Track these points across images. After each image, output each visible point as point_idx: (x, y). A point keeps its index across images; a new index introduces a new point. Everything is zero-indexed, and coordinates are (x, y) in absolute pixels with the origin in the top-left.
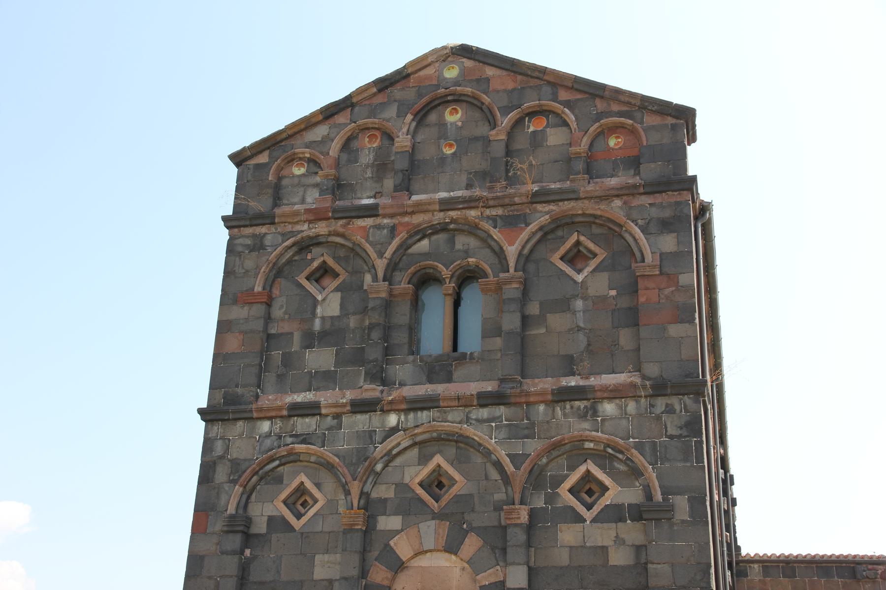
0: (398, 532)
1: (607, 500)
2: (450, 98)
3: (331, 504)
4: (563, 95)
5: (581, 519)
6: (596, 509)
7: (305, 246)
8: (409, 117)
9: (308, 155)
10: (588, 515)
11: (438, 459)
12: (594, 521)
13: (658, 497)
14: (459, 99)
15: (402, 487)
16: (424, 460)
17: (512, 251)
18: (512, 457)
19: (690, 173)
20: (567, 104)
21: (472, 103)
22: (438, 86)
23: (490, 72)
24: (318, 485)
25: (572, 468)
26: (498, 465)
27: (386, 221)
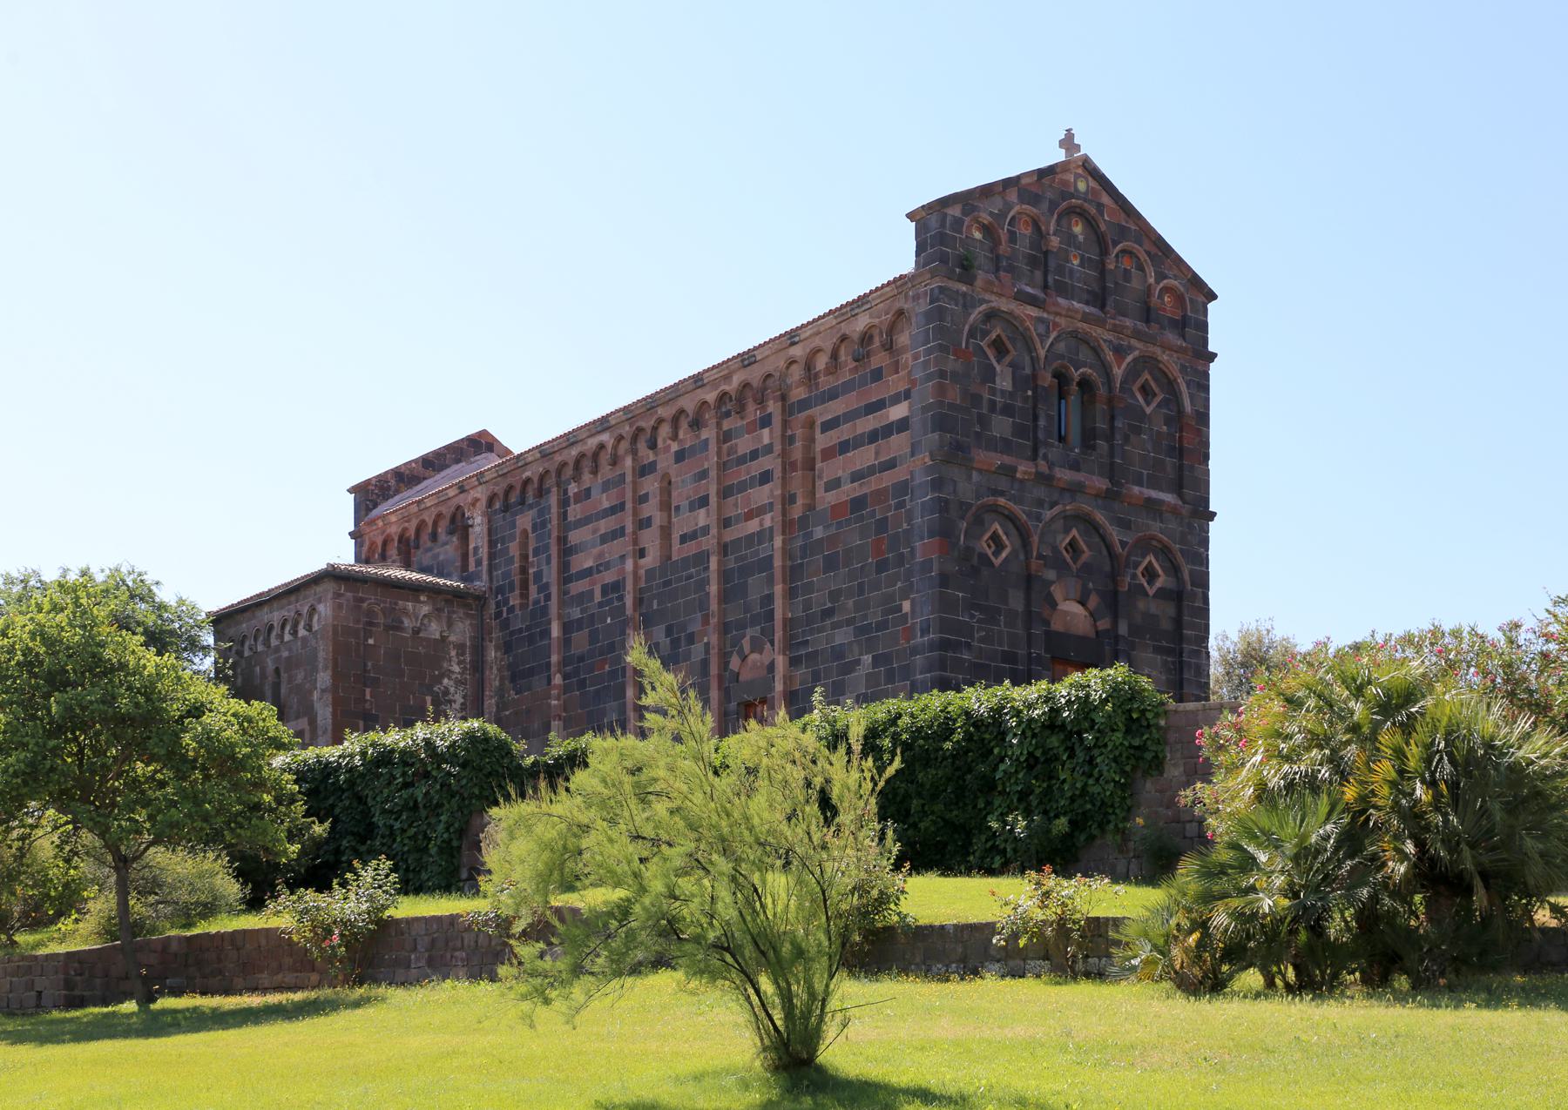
0: (1054, 582)
1: (1159, 583)
2: (1078, 210)
3: (1014, 552)
4: (1147, 245)
5: (1147, 594)
6: (1155, 589)
7: (991, 315)
8: (1055, 216)
9: (985, 222)
10: (1151, 592)
11: (1074, 532)
12: (1155, 596)
13: (1189, 587)
14: (1082, 214)
15: (1055, 549)
16: (1067, 531)
17: (1118, 372)
18: (1121, 541)
19: (1211, 348)
20: (1148, 253)
21: (1090, 223)
22: (1072, 196)
23: (1106, 199)
24: (1006, 534)
25: (1144, 557)
26: (1109, 548)
27: (1045, 315)
